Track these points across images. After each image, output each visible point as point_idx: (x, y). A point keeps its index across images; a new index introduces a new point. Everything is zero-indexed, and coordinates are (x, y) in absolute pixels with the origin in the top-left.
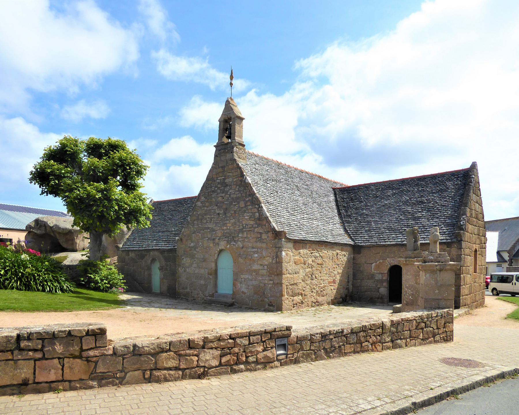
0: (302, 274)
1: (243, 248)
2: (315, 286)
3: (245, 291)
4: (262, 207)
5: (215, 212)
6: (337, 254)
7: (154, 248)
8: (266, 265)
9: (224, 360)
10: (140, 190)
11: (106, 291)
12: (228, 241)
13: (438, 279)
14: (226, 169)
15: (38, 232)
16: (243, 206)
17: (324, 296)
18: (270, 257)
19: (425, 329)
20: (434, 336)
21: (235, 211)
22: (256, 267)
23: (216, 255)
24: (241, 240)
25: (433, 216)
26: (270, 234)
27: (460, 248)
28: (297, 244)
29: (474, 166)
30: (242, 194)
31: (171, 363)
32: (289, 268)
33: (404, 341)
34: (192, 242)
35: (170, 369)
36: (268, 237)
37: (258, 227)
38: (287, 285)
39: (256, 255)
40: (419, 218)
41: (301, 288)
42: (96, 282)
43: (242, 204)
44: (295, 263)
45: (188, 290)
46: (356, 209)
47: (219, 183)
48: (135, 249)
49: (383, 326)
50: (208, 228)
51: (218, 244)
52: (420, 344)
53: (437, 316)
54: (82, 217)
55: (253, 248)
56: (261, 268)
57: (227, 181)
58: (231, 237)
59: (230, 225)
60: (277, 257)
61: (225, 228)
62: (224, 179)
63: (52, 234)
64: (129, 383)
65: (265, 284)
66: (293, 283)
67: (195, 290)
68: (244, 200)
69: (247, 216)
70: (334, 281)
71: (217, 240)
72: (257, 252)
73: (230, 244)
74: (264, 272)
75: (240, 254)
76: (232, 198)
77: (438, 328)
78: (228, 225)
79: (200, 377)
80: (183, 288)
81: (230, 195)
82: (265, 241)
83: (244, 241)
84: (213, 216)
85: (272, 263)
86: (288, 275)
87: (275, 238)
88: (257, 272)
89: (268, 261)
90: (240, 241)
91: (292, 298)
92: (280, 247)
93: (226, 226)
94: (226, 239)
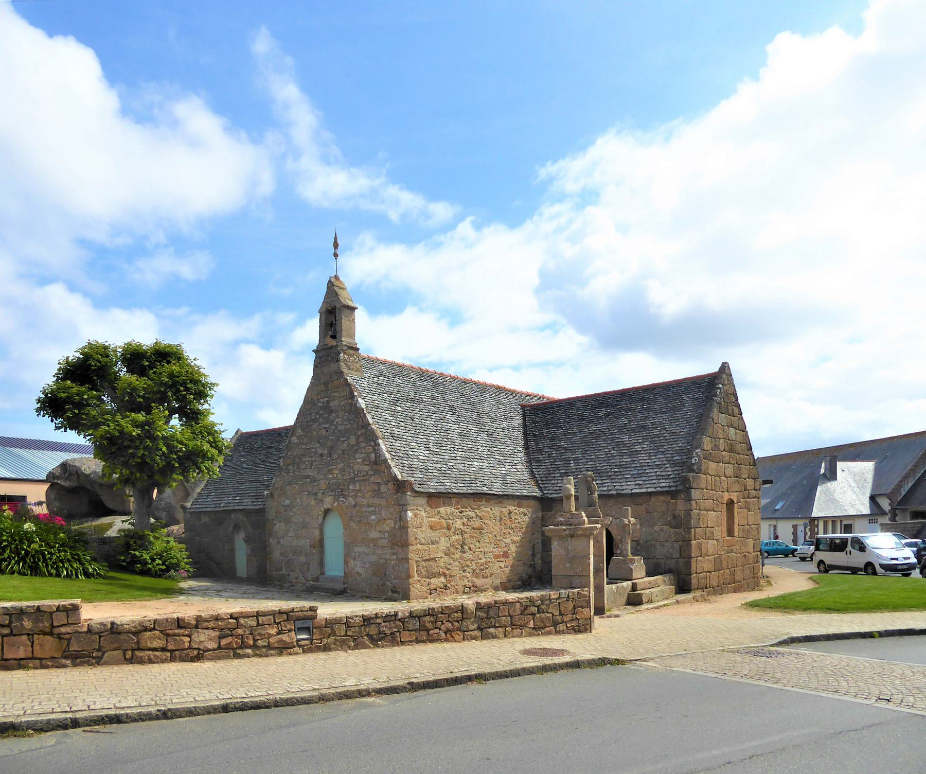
0: (444, 543)
2: (468, 563)
3: (361, 571)
4: (379, 445)
5: (316, 453)
6: (510, 513)
7: (236, 508)
9: (224, 642)
10: (212, 418)
11: (160, 576)
12: (335, 496)
13: (570, 548)
15: (67, 484)
17: (487, 577)
19: (538, 615)
20: (555, 624)
21: (343, 451)
22: (373, 534)
23: (321, 518)
24: (352, 494)
25: (657, 450)
27: (689, 500)
28: (434, 499)
29: (725, 367)
31: (156, 644)
32: (421, 536)
33: (500, 629)
34: (287, 498)
35: (155, 649)
36: (388, 489)
38: (417, 562)
39: (373, 517)
40: (637, 452)
41: (442, 565)
42: (145, 563)
43: (353, 440)
44: (431, 528)
45: (284, 572)
46: (552, 439)
47: (321, 408)
48: (208, 510)
49: (462, 609)
50: (308, 477)
52: (530, 635)
53: (559, 598)
54: (113, 466)
55: (369, 506)
56: (380, 535)
57: (332, 404)
58: (339, 491)
60: (401, 519)
62: (328, 402)
63: (89, 487)
64: (107, 663)
65: (386, 560)
67: (292, 571)
68: (355, 434)
69: (359, 458)
70: (506, 555)
71: (320, 495)
72: (374, 513)
73: (338, 501)
77: (561, 614)
79: (192, 660)
80: (277, 570)
81: (336, 426)
82: (384, 495)
83: (356, 496)
85: (394, 528)
86: (419, 546)
88: (375, 541)
89: (389, 525)
91: (427, 580)
92: (404, 505)
93: (332, 474)
94: (333, 493)
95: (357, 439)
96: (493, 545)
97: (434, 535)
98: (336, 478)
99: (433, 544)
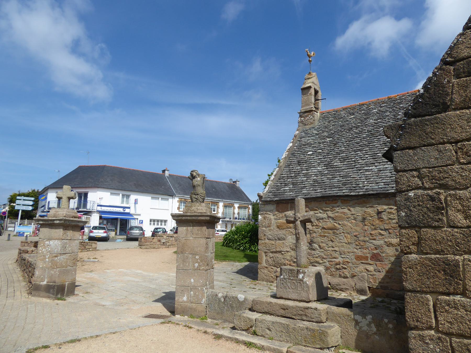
2: (318, 260)
6: (379, 213)
17: (346, 277)
32: (268, 233)
41: (288, 258)
44: (278, 227)
66: (274, 250)
86: (267, 241)
96: (354, 245)
97: (281, 233)
99: (279, 240)
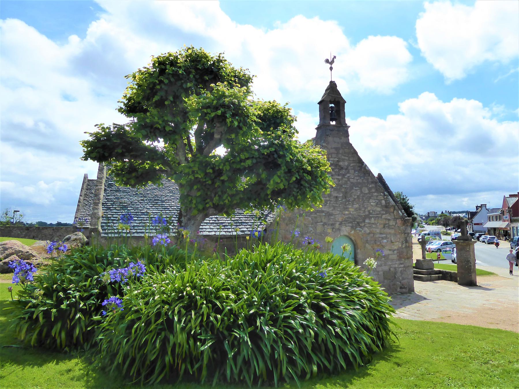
1: (369, 233)
8: (395, 250)
12: (352, 227)
14: (341, 151)
16: (367, 191)
18: (399, 242)
22: (386, 252)
26: (399, 221)
30: (363, 180)
36: (396, 223)
37: (386, 214)
39: (385, 241)
51: (339, 229)
55: (381, 234)
56: (390, 252)
58: (356, 223)
59: (353, 210)
60: (407, 241)
61: (347, 212)
62: (338, 161)
65: (395, 268)
68: (367, 186)
69: (373, 202)
71: (337, 226)
72: (386, 238)
73: (355, 230)
74: (395, 257)
75: (367, 241)
76: (352, 183)
78: (351, 210)
82: (393, 227)
84: (328, 199)
85: (401, 248)
87: (404, 224)
88: (386, 257)
89: (397, 245)
90: (367, 227)
93: (348, 211)
94: (350, 225)
95: (370, 189)
98: (350, 214)
